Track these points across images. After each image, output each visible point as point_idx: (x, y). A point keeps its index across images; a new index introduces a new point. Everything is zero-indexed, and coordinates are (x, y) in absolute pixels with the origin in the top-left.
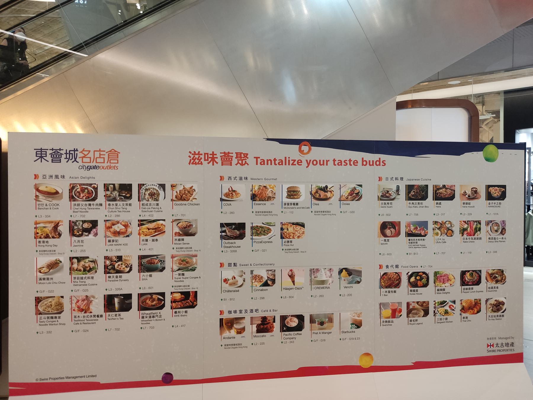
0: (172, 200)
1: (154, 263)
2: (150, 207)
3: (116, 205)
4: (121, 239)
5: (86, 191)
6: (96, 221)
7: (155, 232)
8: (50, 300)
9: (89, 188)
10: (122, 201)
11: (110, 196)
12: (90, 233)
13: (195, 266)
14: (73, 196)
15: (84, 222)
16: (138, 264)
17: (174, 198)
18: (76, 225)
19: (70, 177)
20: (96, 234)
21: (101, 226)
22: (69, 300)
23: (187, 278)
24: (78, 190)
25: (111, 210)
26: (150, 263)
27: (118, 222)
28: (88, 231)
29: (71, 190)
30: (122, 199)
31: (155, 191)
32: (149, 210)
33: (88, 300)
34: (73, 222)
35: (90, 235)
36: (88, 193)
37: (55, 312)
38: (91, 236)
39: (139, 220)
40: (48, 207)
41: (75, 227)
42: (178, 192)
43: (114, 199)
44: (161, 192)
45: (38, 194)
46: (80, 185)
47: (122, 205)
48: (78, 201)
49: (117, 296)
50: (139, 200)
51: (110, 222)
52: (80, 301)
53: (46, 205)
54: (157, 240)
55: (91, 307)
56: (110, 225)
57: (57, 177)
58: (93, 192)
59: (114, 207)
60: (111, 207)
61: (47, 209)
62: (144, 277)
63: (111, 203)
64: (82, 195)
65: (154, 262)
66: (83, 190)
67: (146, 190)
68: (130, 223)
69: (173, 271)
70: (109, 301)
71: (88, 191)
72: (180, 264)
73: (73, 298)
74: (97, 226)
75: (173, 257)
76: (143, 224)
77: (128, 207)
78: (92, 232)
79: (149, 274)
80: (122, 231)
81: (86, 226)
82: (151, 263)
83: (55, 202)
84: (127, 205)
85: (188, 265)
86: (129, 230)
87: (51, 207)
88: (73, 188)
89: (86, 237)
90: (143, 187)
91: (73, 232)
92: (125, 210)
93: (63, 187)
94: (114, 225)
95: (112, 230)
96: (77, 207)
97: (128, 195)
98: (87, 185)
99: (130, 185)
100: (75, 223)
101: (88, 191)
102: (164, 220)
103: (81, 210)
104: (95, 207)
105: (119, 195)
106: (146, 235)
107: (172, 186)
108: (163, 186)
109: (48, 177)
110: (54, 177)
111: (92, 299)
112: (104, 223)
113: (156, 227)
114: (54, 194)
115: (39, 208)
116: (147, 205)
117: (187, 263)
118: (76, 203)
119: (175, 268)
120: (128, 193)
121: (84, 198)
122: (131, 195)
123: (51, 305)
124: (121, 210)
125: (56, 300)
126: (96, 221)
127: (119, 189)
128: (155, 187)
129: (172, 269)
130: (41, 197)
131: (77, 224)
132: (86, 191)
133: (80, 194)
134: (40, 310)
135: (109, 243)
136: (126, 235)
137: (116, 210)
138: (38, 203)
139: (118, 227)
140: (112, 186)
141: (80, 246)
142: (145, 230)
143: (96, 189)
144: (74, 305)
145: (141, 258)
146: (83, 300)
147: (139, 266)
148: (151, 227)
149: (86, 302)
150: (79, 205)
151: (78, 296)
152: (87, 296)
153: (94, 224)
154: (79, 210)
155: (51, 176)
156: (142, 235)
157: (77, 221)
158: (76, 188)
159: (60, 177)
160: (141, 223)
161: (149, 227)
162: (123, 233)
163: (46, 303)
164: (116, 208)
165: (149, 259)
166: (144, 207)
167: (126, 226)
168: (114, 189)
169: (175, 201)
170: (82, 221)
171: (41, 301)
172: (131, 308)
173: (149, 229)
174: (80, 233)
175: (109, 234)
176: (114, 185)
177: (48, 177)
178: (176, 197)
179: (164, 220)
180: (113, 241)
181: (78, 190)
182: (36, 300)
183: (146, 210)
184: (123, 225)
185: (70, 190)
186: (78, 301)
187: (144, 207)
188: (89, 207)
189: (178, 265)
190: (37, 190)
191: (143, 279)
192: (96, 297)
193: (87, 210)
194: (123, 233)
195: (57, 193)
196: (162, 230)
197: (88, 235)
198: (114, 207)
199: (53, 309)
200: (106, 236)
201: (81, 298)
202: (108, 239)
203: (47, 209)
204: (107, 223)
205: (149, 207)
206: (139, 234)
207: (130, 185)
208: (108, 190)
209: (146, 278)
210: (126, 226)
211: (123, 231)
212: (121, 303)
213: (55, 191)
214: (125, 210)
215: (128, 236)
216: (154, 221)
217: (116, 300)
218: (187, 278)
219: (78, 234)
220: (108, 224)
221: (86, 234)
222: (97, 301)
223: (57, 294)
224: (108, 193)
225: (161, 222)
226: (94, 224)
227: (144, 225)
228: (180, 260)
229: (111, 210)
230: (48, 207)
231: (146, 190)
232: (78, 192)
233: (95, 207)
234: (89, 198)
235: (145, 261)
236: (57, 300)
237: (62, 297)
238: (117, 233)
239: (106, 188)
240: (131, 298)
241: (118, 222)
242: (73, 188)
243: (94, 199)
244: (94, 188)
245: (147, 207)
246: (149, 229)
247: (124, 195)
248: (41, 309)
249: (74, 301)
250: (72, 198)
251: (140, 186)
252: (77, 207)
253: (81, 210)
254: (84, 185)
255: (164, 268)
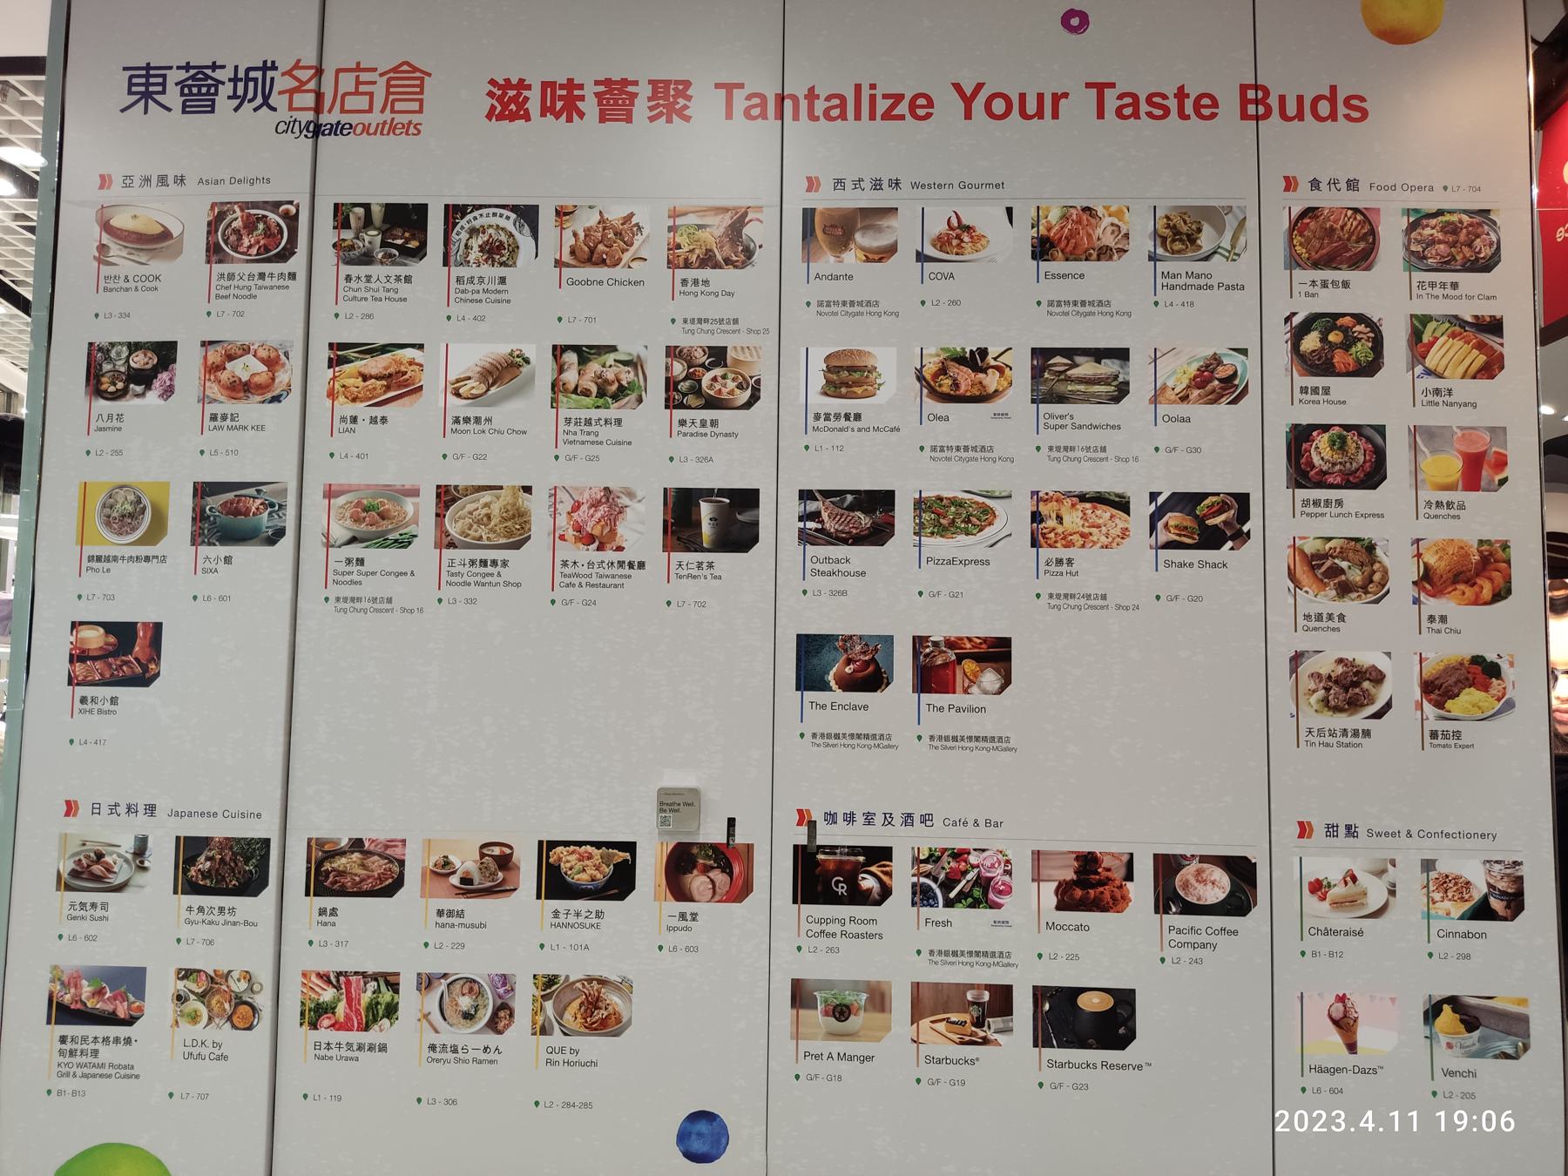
0: (559, 263)
1: (246, 514)
2: (480, 288)
3: (369, 278)
4: (250, 410)
5: (261, 226)
6: (172, 346)
7: (388, 388)
8: (486, 497)
9: (271, 216)
10: (394, 263)
11: (352, 247)
12: (149, 387)
13: (411, 529)
14: (217, 245)
15: (134, 347)
16: (190, 514)
17: (566, 258)
18: (108, 359)
19: (201, 181)
20: (168, 392)
21: (188, 365)
22: (548, 501)
23: (373, 573)
24: (234, 225)
25: (351, 294)
26: (234, 510)
27: (246, 350)
28: (144, 378)
29: (212, 227)
30: (391, 256)
31: (503, 238)
32: (476, 296)
33: (610, 502)
34: (100, 349)
35: (149, 394)
36: (268, 233)
37: (503, 541)
38: (152, 397)
39: (331, 346)
40: (132, 284)
41: (107, 367)
42: (582, 235)
43: (367, 259)
44: (525, 240)
45: (106, 239)
46: (245, 206)
47: (383, 280)
48: (232, 260)
49: (707, 493)
50: (446, 263)
51: (219, 348)
52: (584, 508)
53: (127, 279)
54: (384, 420)
55: (621, 529)
56: (218, 356)
57: (163, 180)
58: (281, 231)
59: (362, 285)
60: (353, 284)
61: (127, 290)
62: (207, 565)
63: (355, 270)
64: (246, 242)
65: (248, 509)
66: (250, 225)
67: (473, 232)
68: (286, 354)
69: (328, 545)
70: (681, 515)
71: (268, 228)
72: (357, 520)
73: (561, 495)
74: (174, 361)
75: (330, 493)
76: (346, 361)
77: (402, 286)
78: (156, 383)
79: (223, 550)
80: (257, 379)
81: (140, 361)
82: (237, 513)
83: (156, 266)
84: (398, 279)
85: (385, 525)
86: (282, 377)
87: (140, 285)
88: (220, 217)
89: (137, 401)
90: (463, 222)
91: (99, 382)
92: (391, 294)
93: (187, 219)
94: (231, 357)
95: (224, 376)
96: (226, 283)
97: (413, 244)
98: (264, 205)
99: (422, 210)
100: (105, 351)
101: (268, 228)
102: (421, 347)
103: (237, 292)
104: (275, 282)
105: (384, 244)
106: (354, 400)
107: (558, 213)
108: (528, 215)
109: (137, 182)
110: (154, 181)
111: (624, 500)
112: (199, 351)
113: (392, 370)
114: (156, 241)
115: (105, 289)
116: (471, 280)
117: (383, 516)
118: (225, 268)
119: (339, 532)
120: (413, 237)
121: (254, 251)
122: (423, 245)
123: (489, 517)
124: (382, 294)
125: (505, 497)
126: (172, 346)
127: (385, 220)
128: (502, 222)
129: (327, 536)
130: (115, 249)
131: (113, 354)
132: (261, 226)
133: (240, 239)
134: (452, 531)
135: (213, 424)
136: (269, 396)
137: (368, 295)
138: (105, 270)
139: (244, 368)
140: (360, 211)
141: (113, 429)
142: (350, 382)
143: (292, 220)
144: (562, 520)
145: (203, 490)
146: (595, 505)
147: (194, 519)
148: (374, 372)
149: (603, 509)
150: (231, 276)
151: (576, 489)
152: (606, 489)
153: (166, 353)
154: (232, 291)
155: (147, 180)
156: (341, 399)
157: (112, 345)
158: (229, 217)
159: (171, 180)
160: (340, 354)
161: (366, 371)
162: (261, 388)
163: (470, 507)
164: (368, 290)
165: (230, 496)
166: (462, 287)
167: (272, 363)
168: (368, 222)
169: (568, 265)
170: (129, 345)
171: (454, 500)
172: (755, 540)
173: (365, 378)
174: (120, 385)
175: (214, 390)
176: (367, 207)
177: (137, 182)
178: (573, 253)
179: (421, 347)
180: (224, 417)
181: (234, 225)
182: (438, 496)
183: (469, 296)
184: (263, 361)
185: (209, 224)
186: (577, 506)
187: (462, 287)
188: (260, 283)
189: (349, 523)
190: (107, 227)
191: (205, 571)
192: (640, 495)
193: (254, 292)
194: (261, 388)
195: (166, 235)
196: (405, 384)
197: (143, 395)
198: (362, 285)
199: (492, 531)
200: (204, 399)
201: (586, 496)
202: (211, 409)
203: (127, 290)
204: (211, 350)
205: (477, 287)
206: (332, 394)
207: (422, 210)
208: (345, 224)
209: (213, 566)
210: (272, 363)
211: (261, 380)
212: (721, 521)
213: (159, 230)
214: (391, 294)
215: (276, 399)
216: (385, 349)
217: (706, 510)
218: (373, 573)
219: (112, 389)
220: (214, 356)
221: (139, 389)
222: (640, 507)
223: (511, 479)
224: (348, 235)
225: (410, 353)
226: (166, 353)
227: (350, 361)
228: (359, 504)
229: (351, 294)
230: (132, 284)
231: (473, 232)
232: (236, 232)
233: (275, 282)
234: (267, 250)
235: (214, 502)
236: (510, 499)
237: (527, 489)
238: (241, 389)
239: (340, 218)
240: (757, 506)
241: (246, 350)
242: (220, 217)
243: (284, 256)
244: (286, 216)
245: (470, 287)
246: (365, 378)
247: (399, 242)
248: (453, 529)
249: (565, 506)
250: (214, 252)
251: (454, 213)
252: (226, 283)
253: (237, 292)
254: (255, 205)
255: (280, 533)
